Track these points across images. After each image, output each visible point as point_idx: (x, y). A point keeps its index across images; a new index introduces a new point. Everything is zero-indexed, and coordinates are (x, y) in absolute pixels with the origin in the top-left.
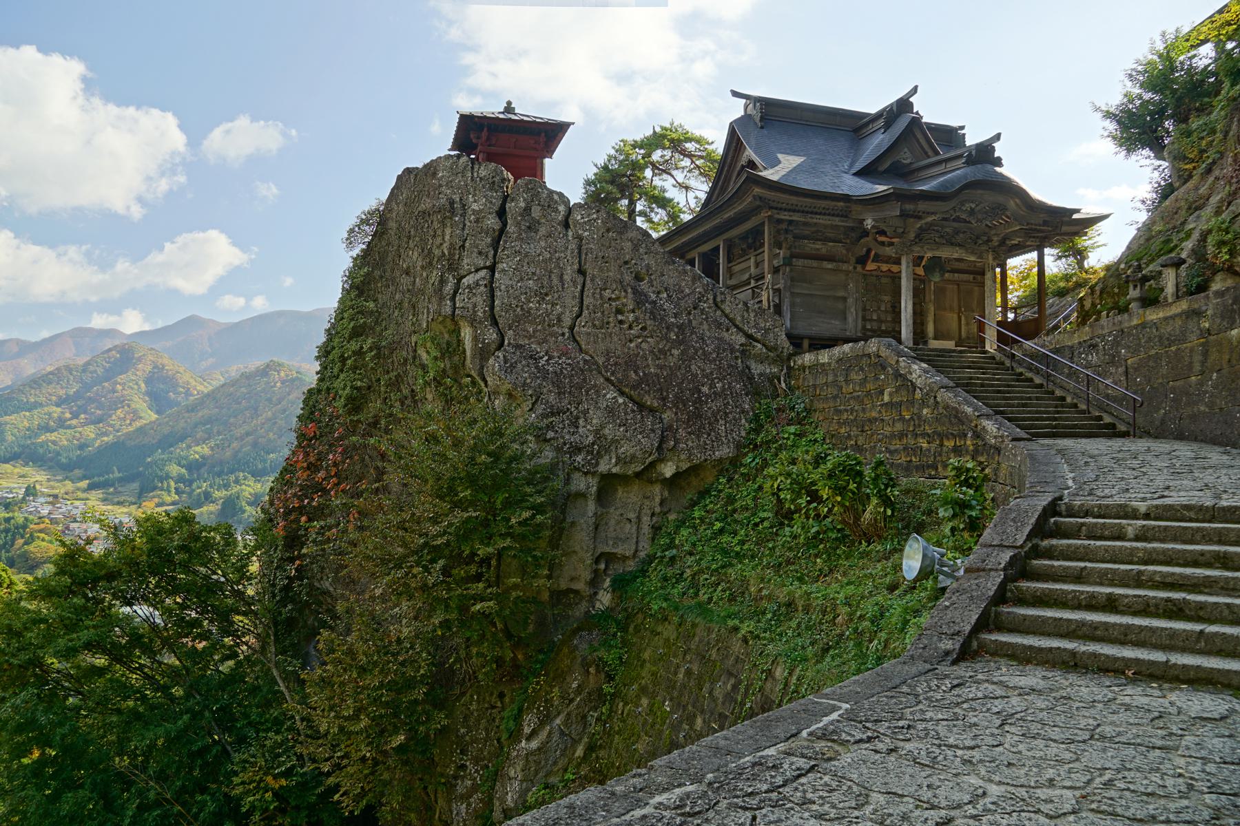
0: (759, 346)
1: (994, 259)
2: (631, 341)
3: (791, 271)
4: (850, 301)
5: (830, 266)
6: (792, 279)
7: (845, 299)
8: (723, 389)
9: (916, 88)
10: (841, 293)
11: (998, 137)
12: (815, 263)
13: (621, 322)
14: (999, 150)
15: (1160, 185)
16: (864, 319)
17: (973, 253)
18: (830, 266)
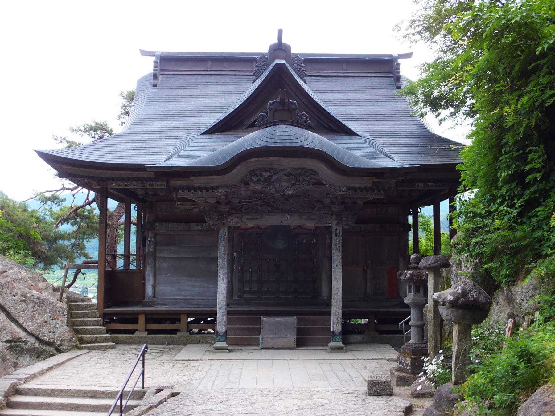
1: (337, 224)
3: (156, 235)
6: (156, 244)
16: (241, 281)
17: (309, 219)
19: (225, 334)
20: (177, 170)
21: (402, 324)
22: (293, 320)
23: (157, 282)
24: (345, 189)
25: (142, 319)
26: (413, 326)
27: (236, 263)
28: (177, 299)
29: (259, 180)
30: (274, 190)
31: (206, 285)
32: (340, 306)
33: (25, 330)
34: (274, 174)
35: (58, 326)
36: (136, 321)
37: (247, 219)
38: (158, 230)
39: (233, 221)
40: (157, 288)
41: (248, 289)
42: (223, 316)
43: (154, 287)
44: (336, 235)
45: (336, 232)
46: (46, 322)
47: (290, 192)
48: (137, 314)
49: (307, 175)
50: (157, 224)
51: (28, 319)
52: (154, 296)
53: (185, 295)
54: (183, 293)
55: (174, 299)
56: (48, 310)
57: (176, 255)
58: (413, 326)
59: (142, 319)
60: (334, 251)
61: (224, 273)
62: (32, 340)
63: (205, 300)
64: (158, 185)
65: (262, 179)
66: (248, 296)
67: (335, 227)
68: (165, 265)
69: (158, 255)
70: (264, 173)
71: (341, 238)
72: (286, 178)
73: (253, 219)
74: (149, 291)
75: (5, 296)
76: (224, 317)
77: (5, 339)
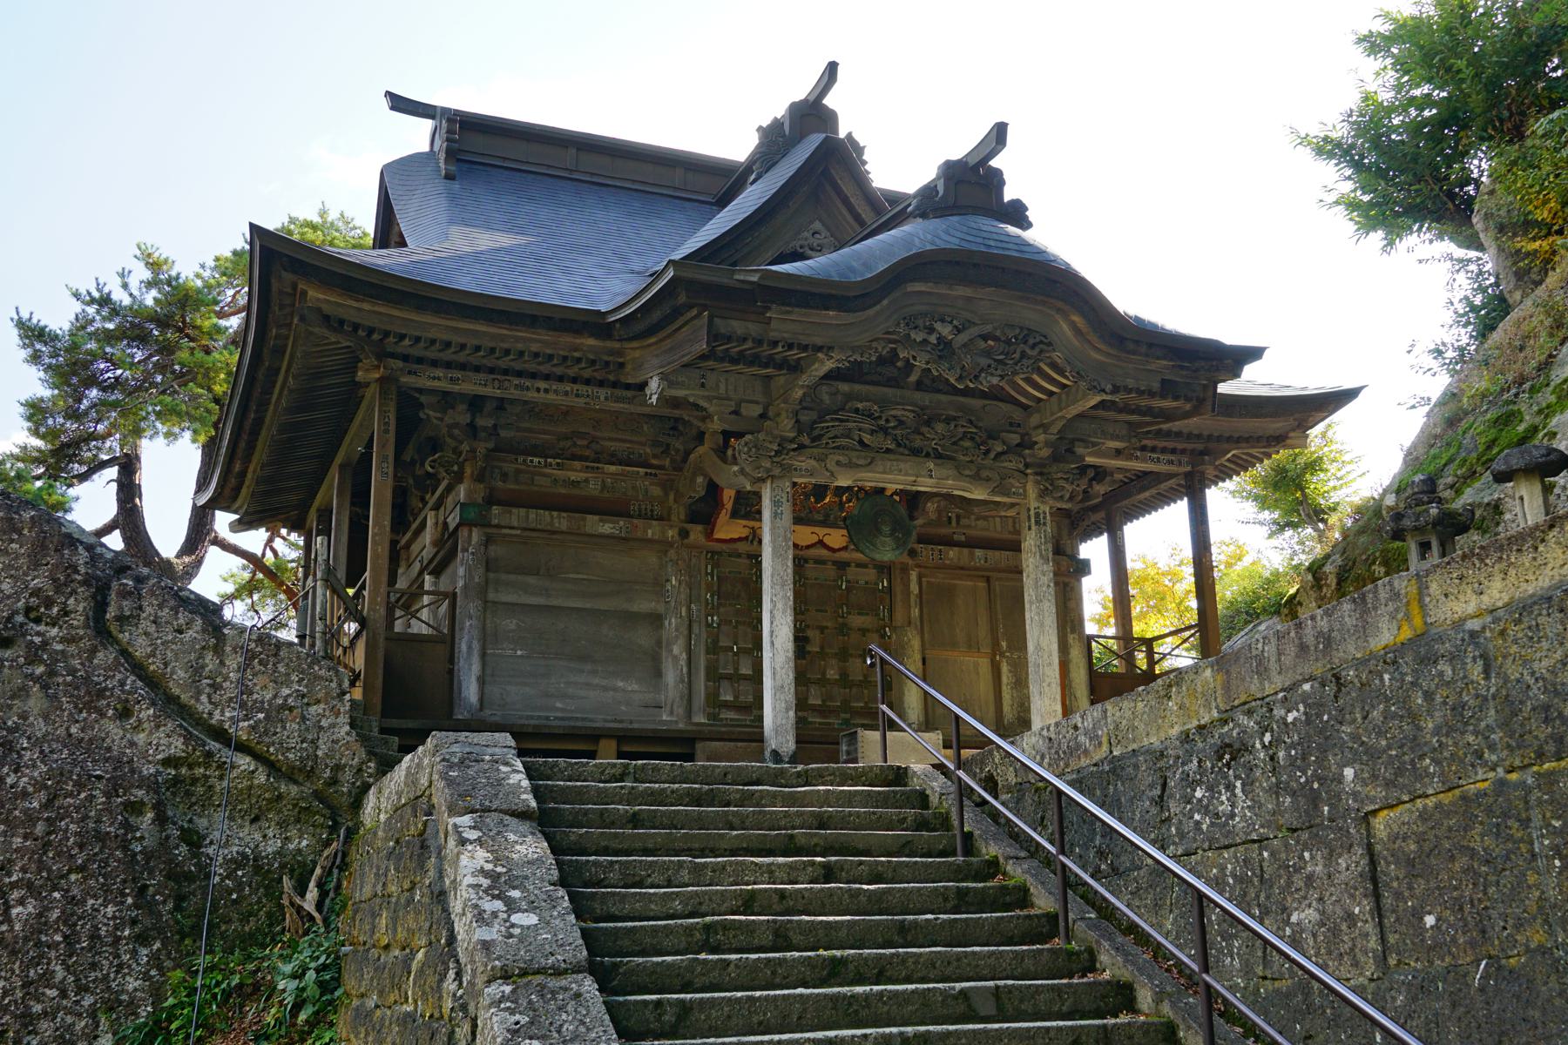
0: (244, 762)
1: (1043, 494)
3: (488, 541)
4: (672, 623)
5: (607, 528)
6: (490, 565)
7: (656, 620)
8: (39, 924)
9: (832, 69)
10: (643, 605)
11: (999, 134)
12: (561, 521)
14: (1019, 176)
15: (1474, 309)
16: (713, 675)
17: (977, 478)
18: (607, 528)
23: (488, 672)
27: (696, 629)
31: (621, 684)
35: (324, 723)
37: (838, 463)
38: (498, 526)
39: (807, 469)
40: (488, 689)
41: (729, 698)
42: (787, 710)
43: (482, 681)
44: (1037, 523)
49: (1031, 341)
50: (495, 510)
52: (481, 709)
54: (559, 705)
57: (541, 601)
64: (538, 390)
65: (933, 339)
66: (731, 715)
68: (510, 624)
69: (491, 596)
70: (938, 326)
73: (851, 465)
74: (470, 691)
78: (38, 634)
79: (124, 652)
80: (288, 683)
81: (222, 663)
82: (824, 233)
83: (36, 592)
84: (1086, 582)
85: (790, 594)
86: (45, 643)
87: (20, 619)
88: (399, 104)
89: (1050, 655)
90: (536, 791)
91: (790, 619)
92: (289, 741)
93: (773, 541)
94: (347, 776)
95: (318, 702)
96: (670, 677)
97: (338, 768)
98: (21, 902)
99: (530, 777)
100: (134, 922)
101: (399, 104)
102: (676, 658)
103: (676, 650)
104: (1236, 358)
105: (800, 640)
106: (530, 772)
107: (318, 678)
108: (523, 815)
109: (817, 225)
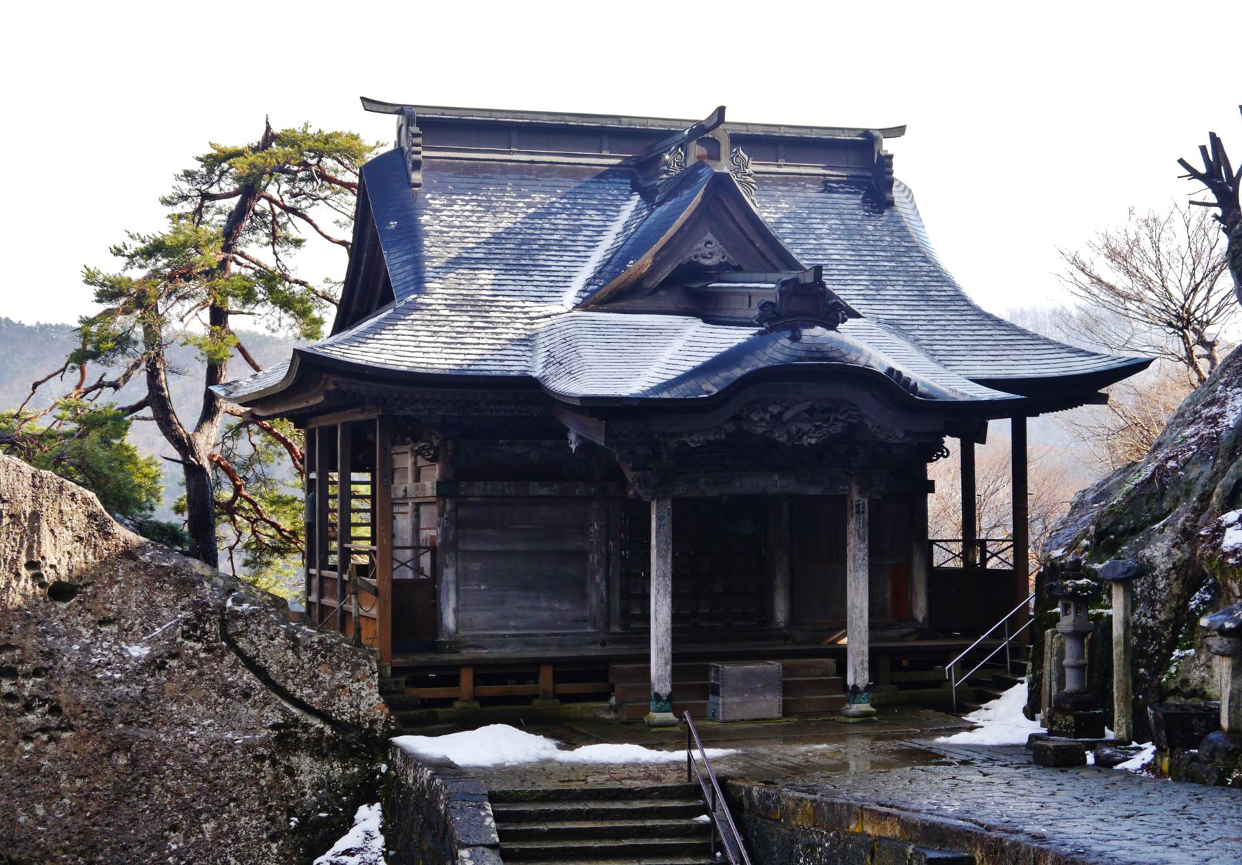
2: (27, 738)
3: (457, 506)
4: (594, 558)
5: (545, 491)
7: (582, 555)
8: (218, 835)
12: (509, 488)
13: (10, 697)
18: (545, 491)
19: (670, 698)
20: (636, 404)
21: (950, 669)
22: (774, 666)
24: (902, 435)
25: (467, 678)
26: (1071, 667)
27: (613, 560)
28: (504, 636)
29: (762, 419)
30: (786, 437)
31: (557, 605)
32: (866, 641)
33: (299, 703)
34: (787, 408)
35: (363, 694)
36: (454, 681)
38: (466, 497)
41: (638, 612)
42: (666, 664)
44: (858, 512)
45: (858, 506)
46: (343, 687)
47: (813, 441)
48: (458, 667)
49: (842, 409)
50: (462, 485)
51: (305, 682)
53: (516, 628)
54: (512, 623)
55: (498, 636)
56: (343, 665)
57: (498, 547)
58: (1071, 667)
59: (467, 678)
60: (852, 541)
61: (666, 585)
62: (317, 723)
63: (557, 635)
67: (856, 498)
69: (461, 546)
70: (771, 409)
71: (866, 516)
72: (806, 416)
74: (449, 620)
75: (255, 639)
76: (669, 667)
77: (271, 723)
78: (191, 648)
79: (240, 653)
80: (339, 669)
81: (299, 658)
82: (715, 242)
83: (187, 622)
84: (932, 500)
85: (669, 583)
86: (195, 654)
87: (180, 640)
88: (370, 104)
89: (862, 611)
90: (500, 832)
91: (669, 600)
92: (343, 707)
93: (658, 546)
94: (379, 726)
95: (358, 681)
96: (594, 600)
97: (373, 722)
98: (207, 821)
99: (496, 819)
100: (268, 829)
101: (370, 104)
102: (597, 586)
103: (598, 579)
104: (983, 441)
105: (676, 617)
106: (498, 817)
107: (358, 665)
108: (493, 847)
109: (709, 237)
